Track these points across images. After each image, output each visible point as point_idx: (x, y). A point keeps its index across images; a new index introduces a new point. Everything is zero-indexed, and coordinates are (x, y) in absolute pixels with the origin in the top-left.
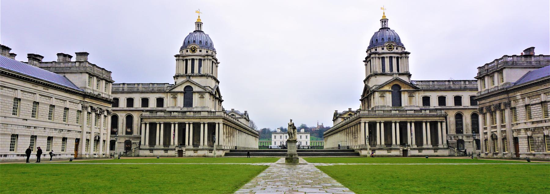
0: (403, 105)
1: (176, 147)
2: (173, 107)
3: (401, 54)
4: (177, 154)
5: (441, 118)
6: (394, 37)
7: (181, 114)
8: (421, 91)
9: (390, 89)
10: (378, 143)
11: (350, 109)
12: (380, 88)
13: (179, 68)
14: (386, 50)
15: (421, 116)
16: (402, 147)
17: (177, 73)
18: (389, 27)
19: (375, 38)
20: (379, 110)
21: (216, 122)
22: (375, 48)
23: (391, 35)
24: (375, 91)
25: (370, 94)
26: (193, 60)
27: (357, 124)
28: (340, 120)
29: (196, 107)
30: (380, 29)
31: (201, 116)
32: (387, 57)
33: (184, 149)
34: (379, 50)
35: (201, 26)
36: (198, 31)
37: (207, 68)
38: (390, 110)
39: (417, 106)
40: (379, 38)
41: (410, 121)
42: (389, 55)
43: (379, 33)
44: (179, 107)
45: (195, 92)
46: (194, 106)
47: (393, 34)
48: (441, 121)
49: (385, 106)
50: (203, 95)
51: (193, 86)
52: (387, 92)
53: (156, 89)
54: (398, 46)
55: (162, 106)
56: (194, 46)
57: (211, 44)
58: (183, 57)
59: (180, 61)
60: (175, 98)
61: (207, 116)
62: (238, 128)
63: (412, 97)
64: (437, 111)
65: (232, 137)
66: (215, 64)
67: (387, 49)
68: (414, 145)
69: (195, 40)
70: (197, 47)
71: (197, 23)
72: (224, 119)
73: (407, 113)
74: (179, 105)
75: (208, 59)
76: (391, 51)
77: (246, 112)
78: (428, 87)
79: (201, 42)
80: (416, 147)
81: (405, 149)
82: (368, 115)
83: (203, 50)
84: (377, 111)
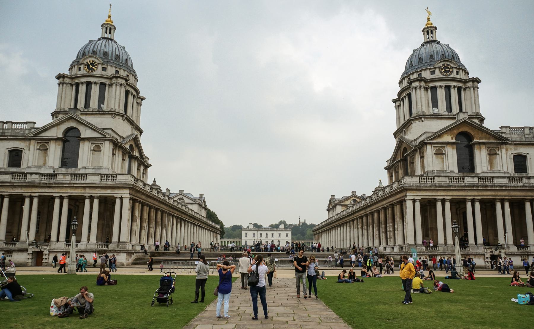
0: (479, 169)
1: (30, 245)
2: (40, 167)
3: (465, 82)
4: (30, 261)
6: (451, 54)
7: (46, 177)
8: (510, 144)
9: (454, 140)
10: (441, 240)
11: (354, 193)
12: (434, 138)
13: (61, 98)
15: (523, 189)
16: (489, 251)
17: (59, 107)
19: (417, 56)
20: (440, 176)
21: (115, 195)
22: (417, 72)
23: (445, 49)
24: (426, 144)
25: (408, 155)
26: (89, 84)
27: (393, 206)
28: (339, 209)
29: (84, 168)
31: (87, 182)
32: (441, 87)
33: (45, 250)
34: (426, 74)
35: (112, 31)
37: (113, 99)
38: (461, 177)
40: (424, 55)
41: (502, 198)
43: (423, 48)
44: (50, 167)
45: (84, 140)
46: (80, 166)
47: (448, 50)
49: (446, 171)
50: (100, 145)
51: (81, 128)
52: (448, 145)
53: (8, 133)
54: (459, 69)
55: (18, 165)
56: (93, 59)
58: (72, 78)
59: (65, 85)
60: (44, 150)
61: (99, 182)
62: (176, 213)
63: (494, 156)
65: (159, 229)
66: (134, 96)
67: (441, 72)
68: (512, 246)
69: (95, 50)
70: (98, 62)
71: (104, 26)
72: (133, 189)
74: (51, 164)
75: (116, 84)
77: (201, 196)
79: (106, 54)
80: (514, 249)
81: (496, 253)
82: (420, 186)
83: (109, 68)
84: (436, 178)
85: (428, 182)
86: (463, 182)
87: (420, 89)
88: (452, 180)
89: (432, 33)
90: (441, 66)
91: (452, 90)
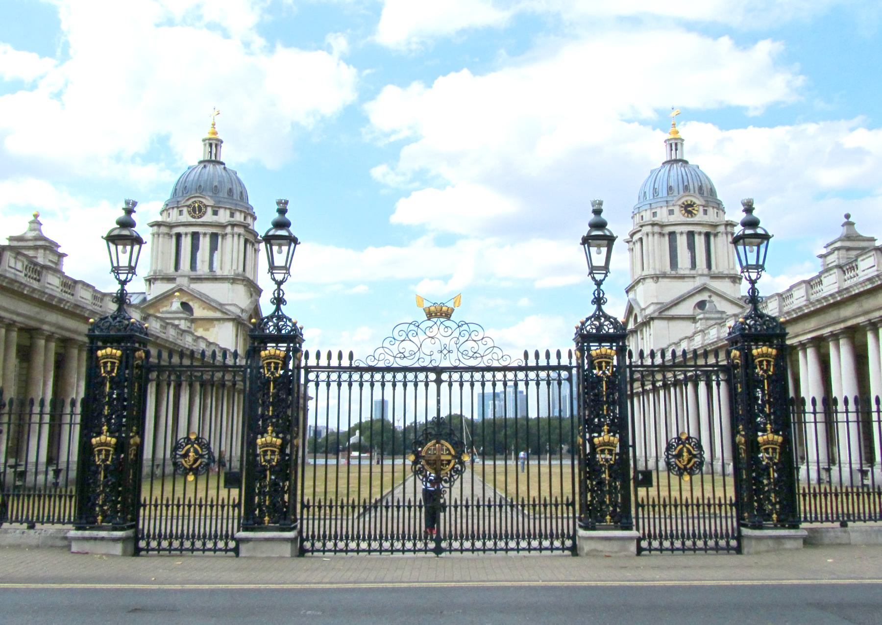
3: (715, 226)
14: (679, 216)
18: (685, 159)
24: (652, 319)
26: (195, 236)
30: (663, 164)
32: (682, 233)
34: (663, 216)
35: (219, 147)
36: (210, 161)
47: (694, 176)
57: (243, 196)
58: (171, 226)
66: (253, 245)
71: (207, 141)
83: (221, 212)
89: (676, 144)
91: (697, 237)
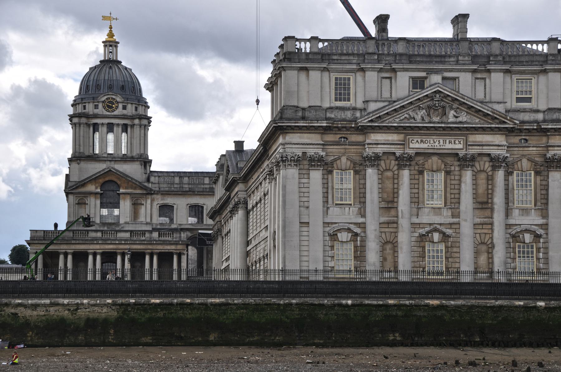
3: (132, 118)
5: (179, 247)
8: (157, 194)
9: (99, 190)
12: (77, 188)
14: (101, 110)
22: (82, 103)
23: (114, 78)
32: (103, 124)
34: (90, 108)
39: (147, 224)
41: (122, 251)
42: (106, 121)
48: (178, 251)
52: (92, 195)
63: (140, 206)
64: (173, 234)
73: (118, 237)
76: (112, 114)
78: (171, 188)
82: (44, 240)
85: (53, 236)
86: (88, 236)
87: (80, 126)
88: (77, 235)
90: (105, 101)
